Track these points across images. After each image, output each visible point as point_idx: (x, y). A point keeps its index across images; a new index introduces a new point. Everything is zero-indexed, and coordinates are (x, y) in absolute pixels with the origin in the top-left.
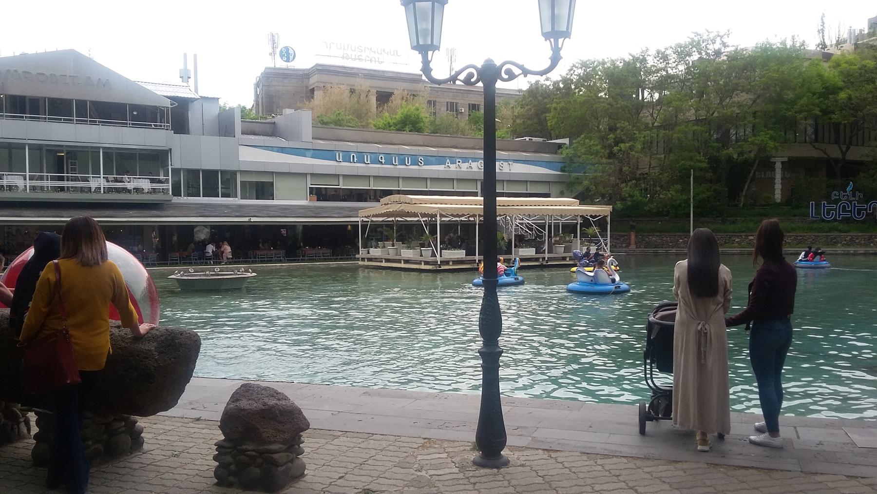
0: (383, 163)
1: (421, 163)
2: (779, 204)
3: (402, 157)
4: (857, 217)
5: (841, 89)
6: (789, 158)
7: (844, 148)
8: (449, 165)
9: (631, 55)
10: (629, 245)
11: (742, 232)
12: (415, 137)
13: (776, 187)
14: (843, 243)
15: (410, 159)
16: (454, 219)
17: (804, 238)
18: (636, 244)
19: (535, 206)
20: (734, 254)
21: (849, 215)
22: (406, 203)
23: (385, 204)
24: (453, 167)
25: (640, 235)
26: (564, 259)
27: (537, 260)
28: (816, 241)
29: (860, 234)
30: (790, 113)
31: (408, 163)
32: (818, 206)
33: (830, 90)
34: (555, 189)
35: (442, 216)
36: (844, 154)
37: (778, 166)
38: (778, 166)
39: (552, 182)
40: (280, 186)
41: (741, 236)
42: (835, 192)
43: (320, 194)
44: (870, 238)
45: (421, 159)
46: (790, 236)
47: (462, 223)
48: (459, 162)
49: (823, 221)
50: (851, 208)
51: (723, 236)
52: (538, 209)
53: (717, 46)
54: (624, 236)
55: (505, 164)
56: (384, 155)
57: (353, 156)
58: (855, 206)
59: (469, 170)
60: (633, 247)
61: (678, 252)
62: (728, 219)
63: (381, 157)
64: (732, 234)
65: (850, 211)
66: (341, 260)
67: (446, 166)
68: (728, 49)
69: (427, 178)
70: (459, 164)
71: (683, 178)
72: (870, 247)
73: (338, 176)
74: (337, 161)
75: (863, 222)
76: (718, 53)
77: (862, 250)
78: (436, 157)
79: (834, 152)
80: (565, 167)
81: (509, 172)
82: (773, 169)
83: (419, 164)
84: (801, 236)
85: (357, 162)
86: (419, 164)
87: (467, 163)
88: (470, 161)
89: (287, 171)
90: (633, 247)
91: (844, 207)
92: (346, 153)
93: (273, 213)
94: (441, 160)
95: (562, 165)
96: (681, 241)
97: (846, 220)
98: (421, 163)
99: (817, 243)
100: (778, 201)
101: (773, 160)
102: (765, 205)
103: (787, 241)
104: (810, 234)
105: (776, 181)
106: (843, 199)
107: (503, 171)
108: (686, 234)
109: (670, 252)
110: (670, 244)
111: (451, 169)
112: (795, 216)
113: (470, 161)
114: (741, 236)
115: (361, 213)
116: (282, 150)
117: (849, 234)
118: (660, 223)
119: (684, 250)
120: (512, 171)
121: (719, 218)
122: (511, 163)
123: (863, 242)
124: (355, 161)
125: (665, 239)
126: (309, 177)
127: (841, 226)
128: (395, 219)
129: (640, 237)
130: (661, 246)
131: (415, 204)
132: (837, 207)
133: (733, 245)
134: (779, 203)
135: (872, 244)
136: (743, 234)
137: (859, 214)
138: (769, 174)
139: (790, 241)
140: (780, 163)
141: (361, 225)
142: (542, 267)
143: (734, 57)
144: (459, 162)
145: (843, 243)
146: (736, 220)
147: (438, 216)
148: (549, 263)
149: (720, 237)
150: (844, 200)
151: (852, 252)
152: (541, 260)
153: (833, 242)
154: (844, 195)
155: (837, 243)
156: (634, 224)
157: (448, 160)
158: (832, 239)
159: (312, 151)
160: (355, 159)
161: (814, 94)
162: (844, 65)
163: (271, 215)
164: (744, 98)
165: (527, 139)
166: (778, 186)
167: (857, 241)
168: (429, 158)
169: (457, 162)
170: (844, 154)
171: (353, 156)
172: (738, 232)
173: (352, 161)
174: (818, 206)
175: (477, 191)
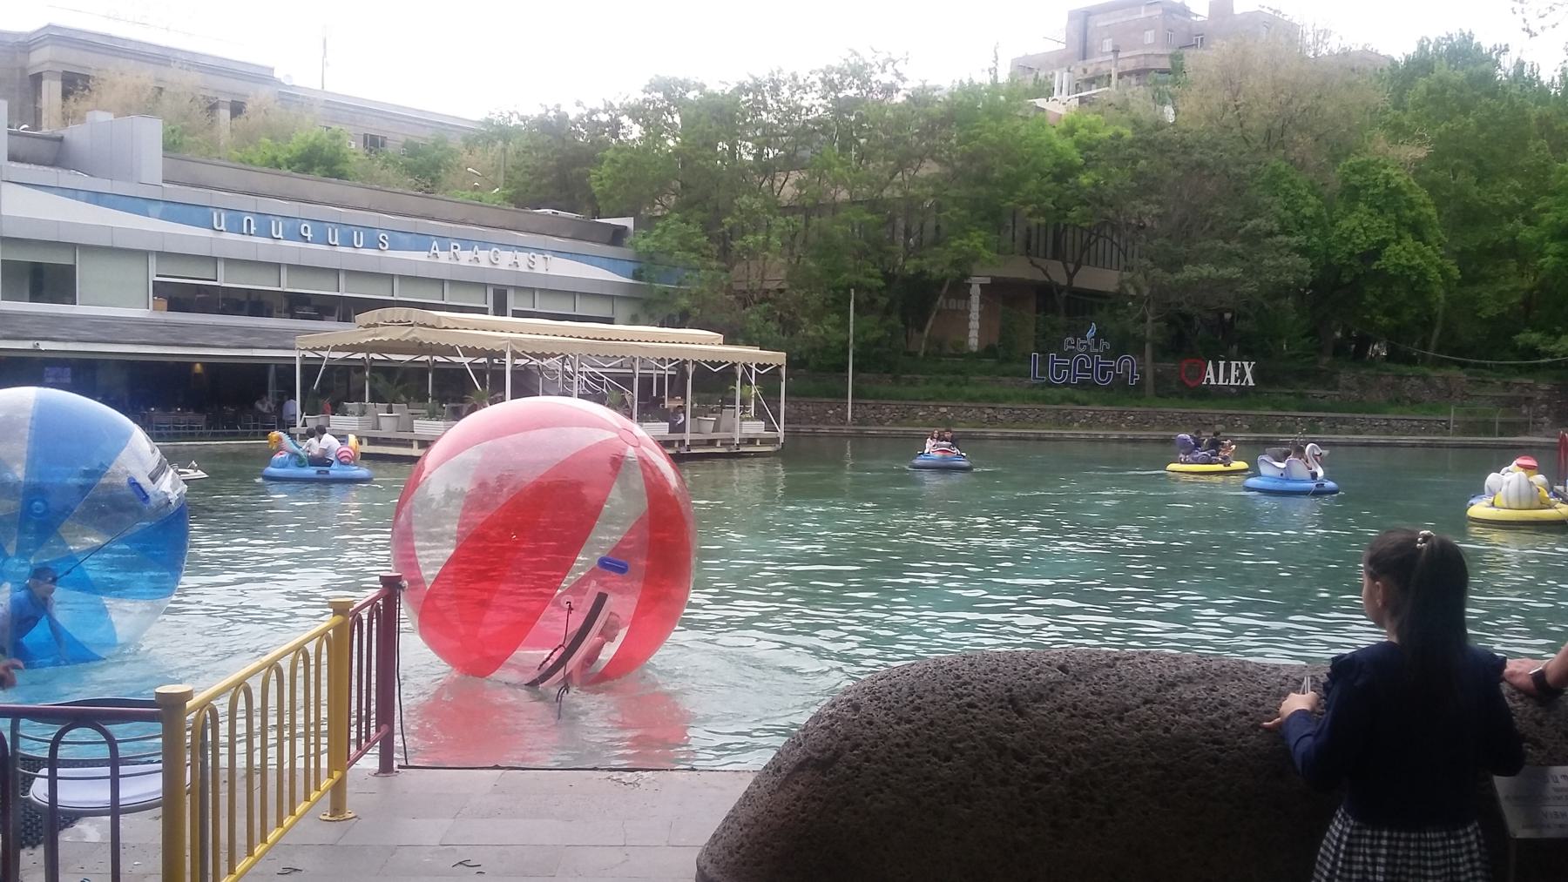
0: (309, 239)
1: (384, 245)
2: (972, 356)
4: (1099, 381)
5: (1080, 169)
6: (994, 279)
7: (1071, 267)
8: (437, 251)
9: (752, 77)
11: (930, 399)
12: (333, 188)
13: (971, 327)
15: (362, 234)
22: (425, 325)
23: (368, 326)
24: (444, 257)
26: (712, 443)
29: (1107, 408)
30: (1010, 203)
31: (359, 243)
32: (1044, 362)
33: (1064, 172)
34: (622, 310)
35: (515, 355)
36: (1071, 276)
37: (975, 292)
38: (975, 292)
39: (617, 296)
40: (87, 274)
41: (928, 407)
42: (1070, 339)
43: (178, 298)
44: (1121, 414)
45: (384, 238)
47: (437, 366)
48: (456, 247)
49: (1050, 385)
52: (677, 348)
53: (887, 78)
56: (312, 223)
57: (249, 220)
58: (1098, 363)
63: (306, 228)
64: (913, 403)
65: (1091, 371)
66: (235, 436)
68: (908, 85)
69: (393, 275)
71: (839, 305)
74: (214, 229)
75: (1109, 389)
76: (889, 90)
77: (1083, 433)
78: (410, 236)
79: (1057, 273)
81: (545, 272)
82: (968, 297)
84: (1019, 409)
85: (256, 234)
88: (476, 247)
89: (110, 245)
92: (233, 213)
93: (83, 332)
94: (421, 241)
96: (831, 412)
97: (1082, 384)
98: (384, 245)
100: (975, 349)
104: (1032, 406)
105: (972, 316)
106: (1082, 350)
108: (839, 401)
111: (439, 261)
112: (1005, 375)
113: (476, 247)
114: (928, 407)
115: (300, 341)
116: (96, 198)
117: (1089, 408)
121: (889, 375)
122: (548, 256)
123: (1111, 421)
124: (252, 232)
125: (804, 407)
126: (153, 261)
127: (1079, 395)
128: (368, 356)
131: (446, 328)
134: (977, 353)
137: (1103, 375)
138: (961, 305)
139: (1003, 417)
141: (302, 366)
143: (919, 100)
144: (456, 247)
147: (508, 355)
148: (692, 451)
152: (676, 445)
153: (1065, 421)
155: (1073, 421)
157: (435, 243)
158: (1065, 416)
159: (162, 205)
160: (253, 229)
161: (1044, 175)
162: (1084, 132)
163: (81, 337)
164: (929, 169)
165: (550, 211)
166: (974, 324)
167: (1102, 419)
170: (1071, 276)
171: (249, 220)
173: (245, 231)
174: (1044, 362)
175: (485, 306)
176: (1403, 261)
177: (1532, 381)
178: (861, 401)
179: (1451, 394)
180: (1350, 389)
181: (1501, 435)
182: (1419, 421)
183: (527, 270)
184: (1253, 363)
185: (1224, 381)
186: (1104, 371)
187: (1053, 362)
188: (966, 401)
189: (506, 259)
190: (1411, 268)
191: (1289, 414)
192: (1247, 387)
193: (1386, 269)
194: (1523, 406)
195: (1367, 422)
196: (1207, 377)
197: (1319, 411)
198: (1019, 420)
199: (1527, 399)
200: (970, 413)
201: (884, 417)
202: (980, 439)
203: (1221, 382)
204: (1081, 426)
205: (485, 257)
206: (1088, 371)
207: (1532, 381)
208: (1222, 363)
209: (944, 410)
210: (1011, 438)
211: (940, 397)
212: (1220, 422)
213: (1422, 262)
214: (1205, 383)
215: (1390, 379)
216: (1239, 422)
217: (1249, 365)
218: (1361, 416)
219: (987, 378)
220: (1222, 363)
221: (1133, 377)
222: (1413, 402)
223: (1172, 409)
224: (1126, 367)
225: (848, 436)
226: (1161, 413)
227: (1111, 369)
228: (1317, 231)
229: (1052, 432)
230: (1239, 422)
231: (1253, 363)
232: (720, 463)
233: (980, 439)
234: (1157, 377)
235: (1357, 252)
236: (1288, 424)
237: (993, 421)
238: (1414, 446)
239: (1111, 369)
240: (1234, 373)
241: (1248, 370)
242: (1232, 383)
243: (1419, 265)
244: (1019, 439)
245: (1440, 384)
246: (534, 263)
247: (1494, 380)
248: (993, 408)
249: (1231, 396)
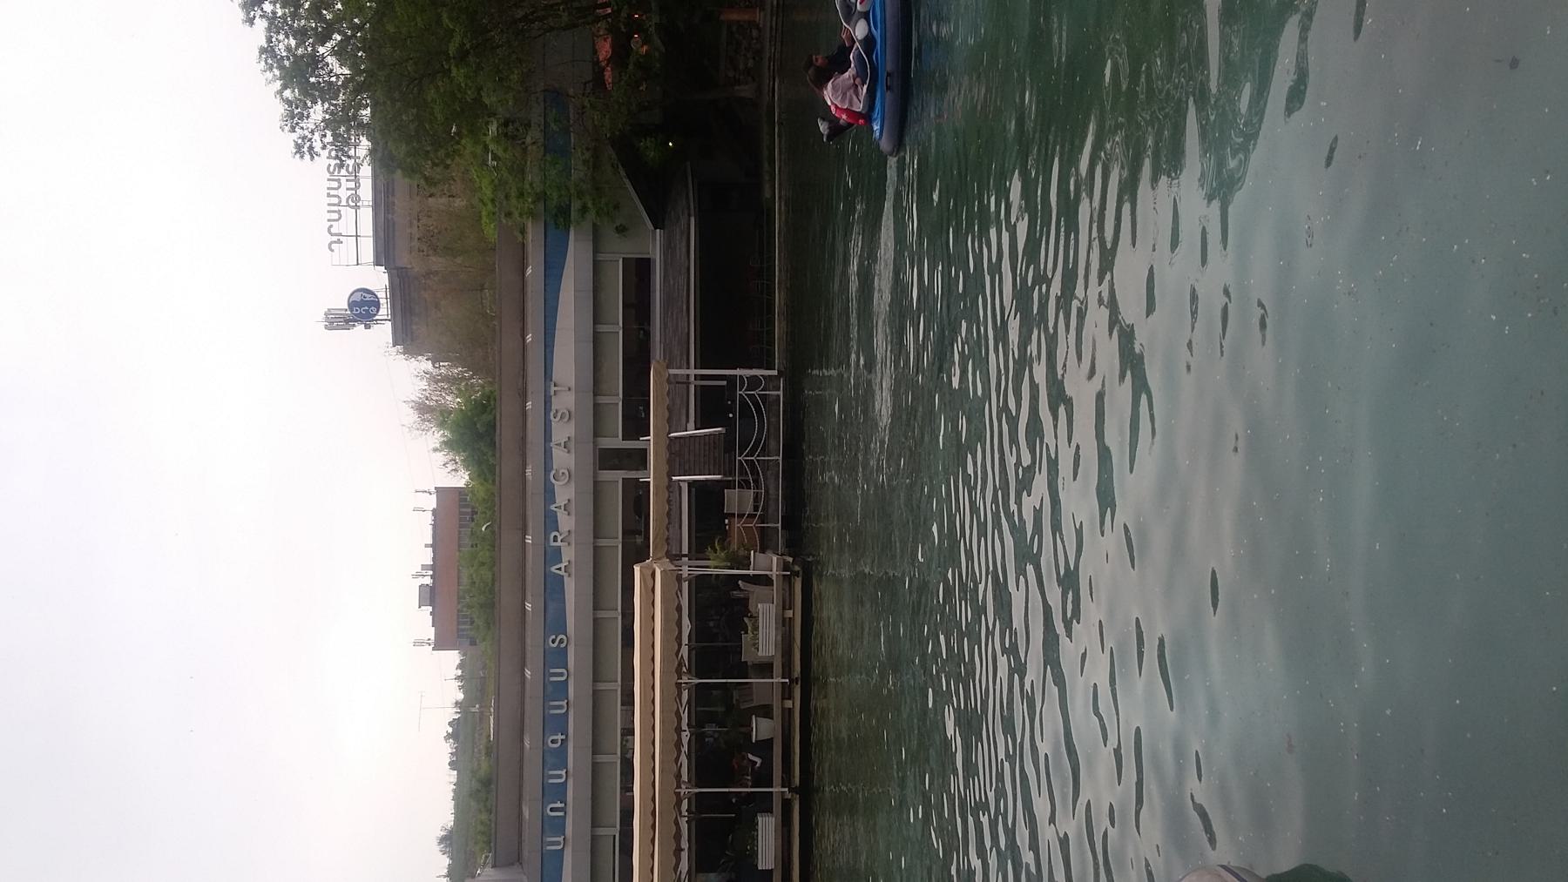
0: (563, 737)
1: (561, 641)
3: (550, 689)
8: (562, 566)
15: (552, 671)
16: (685, 748)
19: (653, 702)
24: (568, 554)
27: (787, 805)
31: (561, 675)
39: (596, 251)
45: (553, 642)
48: (555, 539)
55: (556, 404)
57: (552, 810)
59: (573, 512)
63: (553, 742)
67: (567, 574)
70: (559, 540)
73: (594, 838)
83: (563, 645)
86: (563, 645)
87: (558, 514)
88: (553, 507)
92: (546, 827)
94: (553, 587)
107: (573, 409)
111: (573, 560)
113: (553, 507)
120: (572, 384)
122: (553, 389)
124: (563, 805)
142: (807, 791)
148: (797, 781)
157: (553, 569)
160: (559, 805)
168: (548, 622)
169: (555, 544)
171: (552, 810)
173: (561, 814)
183: (573, 422)
189: (563, 459)
205: (564, 493)
232: (818, 703)
246: (563, 413)
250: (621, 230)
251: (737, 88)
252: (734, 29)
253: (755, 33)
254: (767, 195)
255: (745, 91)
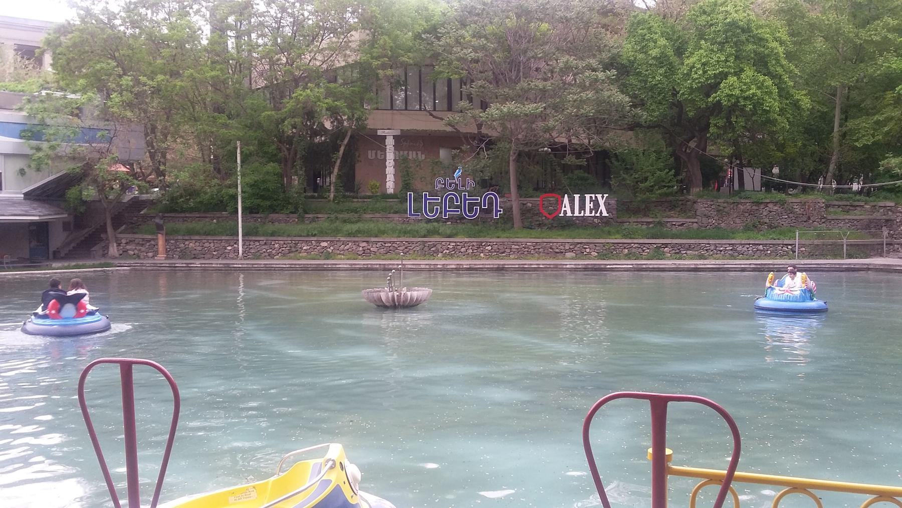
4: (468, 216)
10: (156, 253)
11: (315, 235)
14: (444, 252)
17: (393, 245)
18: (167, 252)
20: (282, 269)
21: (458, 211)
25: (173, 240)
28: (410, 249)
29: (466, 240)
37: (390, 142)
38: (390, 142)
44: (480, 244)
46: (376, 242)
50: (461, 202)
51: (286, 242)
54: (149, 241)
58: (465, 200)
60: (161, 258)
61: (203, 266)
62: (307, 216)
65: (459, 207)
72: (480, 258)
75: (475, 222)
80: (24, 131)
84: (390, 242)
90: (161, 258)
91: (451, 200)
95: (21, 128)
96: (229, 248)
99: (411, 252)
101: (380, 133)
102: (369, 197)
103: (372, 249)
109: (192, 265)
110: (215, 253)
112: (396, 212)
118: (215, 221)
119: (212, 264)
123: (471, 251)
125: (207, 245)
129: (172, 242)
130: (203, 256)
132: (442, 200)
133: (301, 254)
135: (482, 255)
136: (312, 239)
137: (470, 210)
140: (392, 137)
145: (444, 252)
146: (317, 218)
149: (282, 242)
150: (450, 191)
151: (439, 266)
154: (450, 184)
155: (437, 252)
156: (161, 222)
166: (390, 170)
167: (463, 250)
172: (308, 236)
176: (737, 92)
177: (892, 204)
178: (254, 238)
179: (809, 218)
180: (708, 217)
181: (850, 256)
182: (764, 245)
184: (606, 195)
185: (580, 213)
186: (471, 206)
187: (426, 199)
188: (345, 236)
190: (745, 99)
191: (635, 241)
192: (601, 217)
193: (719, 102)
194: (884, 228)
195: (712, 248)
196: (563, 209)
197: (667, 238)
198: (389, 252)
199: (887, 221)
200: (348, 247)
201: (274, 252)
202: (332, 270)
203: (577, 214)
204: (445, 256)
206: (458, 207)
207: (892, 204)
208: (577, 197)
209: (324, 244)
210: (360, 269)
211: (322, 233)
212: (570, 250)
213: (759, 92)
214: (562, 215)
215: (748, 206)
216: (588, 250)
217: (603, 197)
218: (705, 241)
219: (378, 215)
220: (577, 197)
221: (497, 211)
222: (770, 227)
223: (527, 239)
224: (491, 204)
225: (241, 270)
226: (517, 243)
227: (437, 204)
228: (662, 71)
229: (423, 263)
230: (588, 250)
231: (606, 195)
233: (332, 270)
234: (525, 212)
235: (695, 86)
236: (634, 250)
237: (366, 254)
238: (743, 270)
239: (437, 204)
240: (588, 205)
241: (601, 202)
242: (588, 214)
243: (753, 94)
244: (368, 269)
245: (797, 209)
247: (862, 204)
248: (367, 242)
249: (595, 226)
250: (22, 172)
251: (115, 245)
252: (153, 242)
253: (150, 254)
254: (54, 265)
255: (113, 250)
